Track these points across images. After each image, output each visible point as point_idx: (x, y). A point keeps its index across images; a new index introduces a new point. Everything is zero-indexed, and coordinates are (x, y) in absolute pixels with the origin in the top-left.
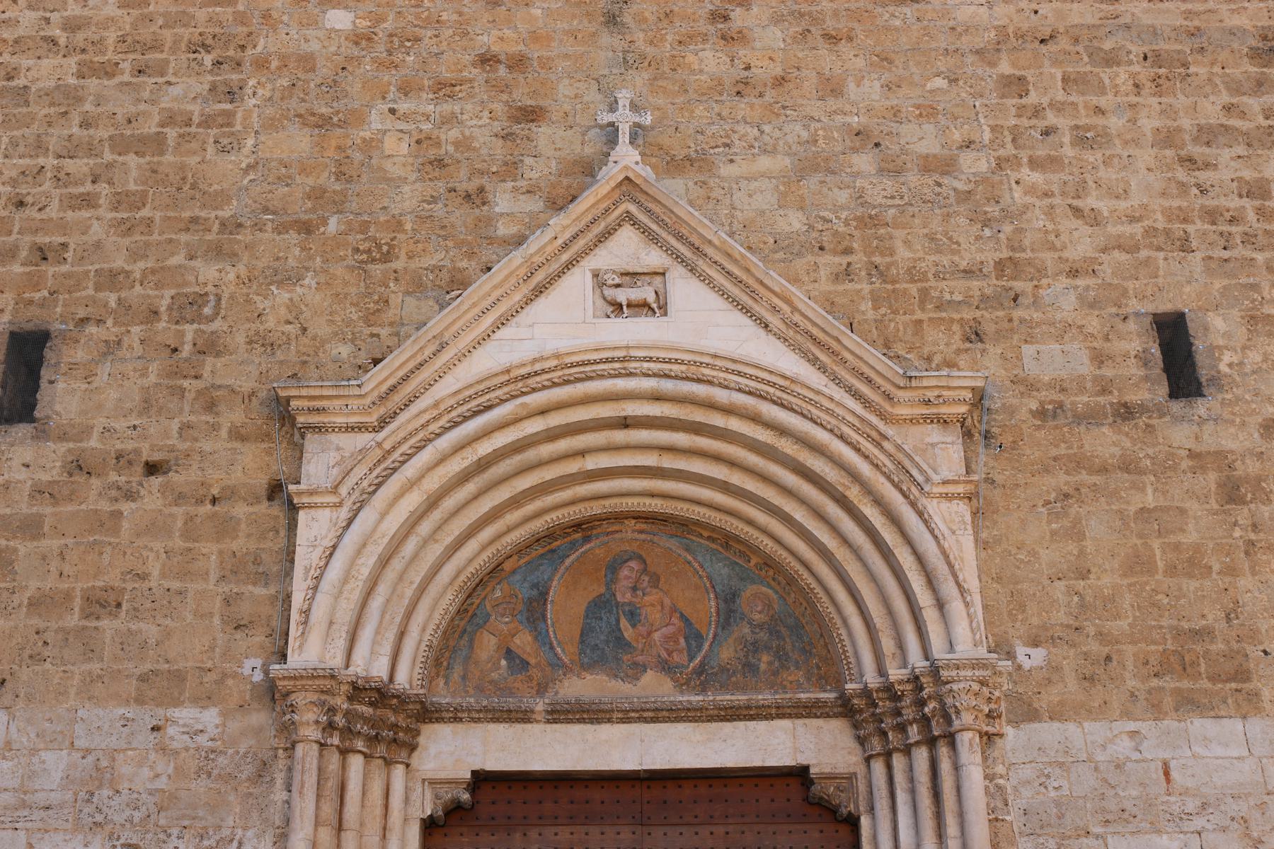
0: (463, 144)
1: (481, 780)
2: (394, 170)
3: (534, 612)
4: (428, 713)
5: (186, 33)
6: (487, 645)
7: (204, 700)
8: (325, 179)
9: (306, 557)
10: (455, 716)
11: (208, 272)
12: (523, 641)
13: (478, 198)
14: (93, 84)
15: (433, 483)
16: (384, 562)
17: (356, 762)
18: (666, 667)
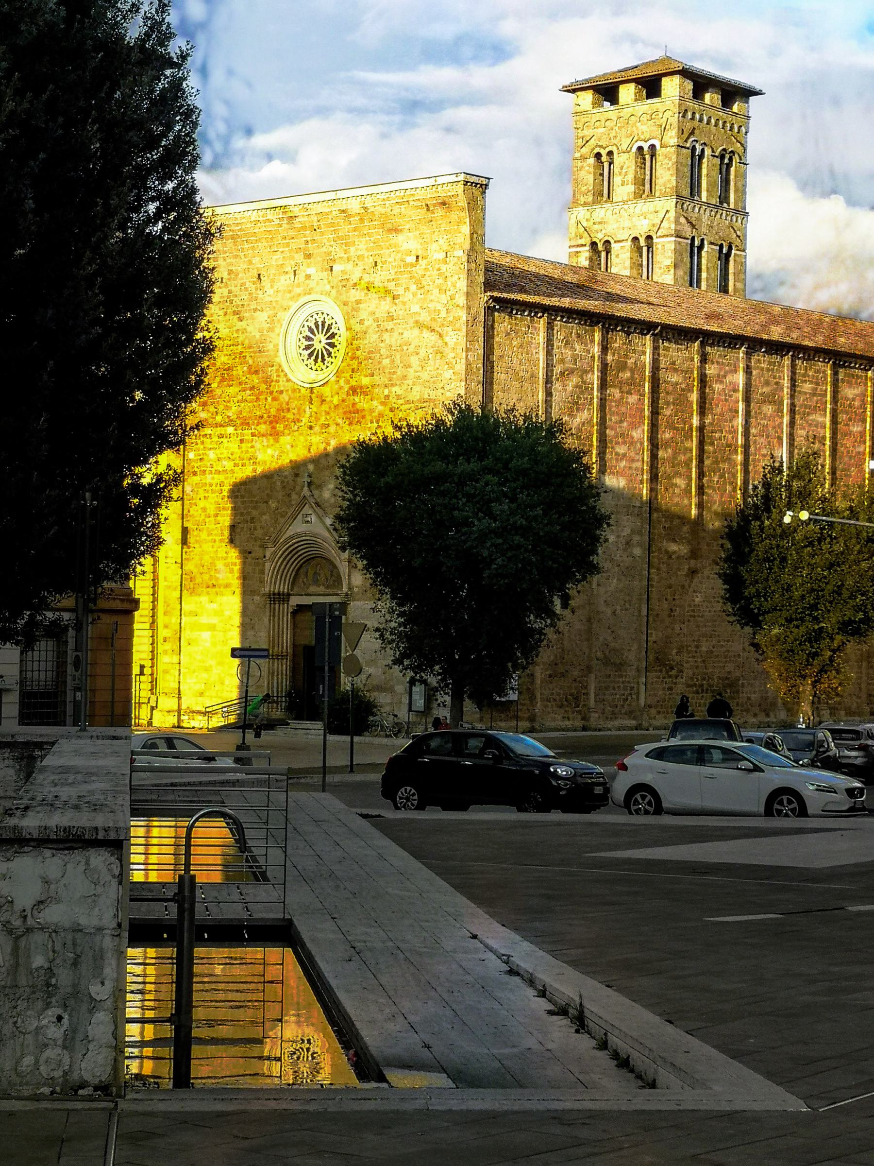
0: (288, 482)
1: (298, 605)
2: (278, 489)
3: (307, 576)
4: (289, 595)
5: (248, 455)
6: (301, 580)
7: (258, 595)
8: (268, 491)
9: (266, 571)
10: (294, 595)
11: (254, 513)
12: (305, 580)
13: (289, 495)
14: (236, 468)
15: (284, 556)
16: (278, 570)
17: (277, 605)
18: (324, 585)
